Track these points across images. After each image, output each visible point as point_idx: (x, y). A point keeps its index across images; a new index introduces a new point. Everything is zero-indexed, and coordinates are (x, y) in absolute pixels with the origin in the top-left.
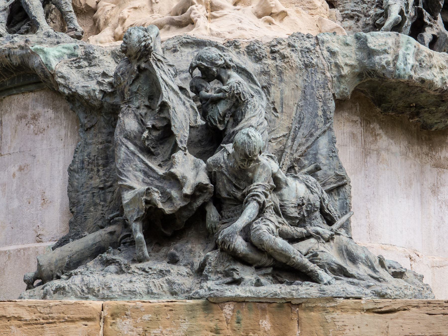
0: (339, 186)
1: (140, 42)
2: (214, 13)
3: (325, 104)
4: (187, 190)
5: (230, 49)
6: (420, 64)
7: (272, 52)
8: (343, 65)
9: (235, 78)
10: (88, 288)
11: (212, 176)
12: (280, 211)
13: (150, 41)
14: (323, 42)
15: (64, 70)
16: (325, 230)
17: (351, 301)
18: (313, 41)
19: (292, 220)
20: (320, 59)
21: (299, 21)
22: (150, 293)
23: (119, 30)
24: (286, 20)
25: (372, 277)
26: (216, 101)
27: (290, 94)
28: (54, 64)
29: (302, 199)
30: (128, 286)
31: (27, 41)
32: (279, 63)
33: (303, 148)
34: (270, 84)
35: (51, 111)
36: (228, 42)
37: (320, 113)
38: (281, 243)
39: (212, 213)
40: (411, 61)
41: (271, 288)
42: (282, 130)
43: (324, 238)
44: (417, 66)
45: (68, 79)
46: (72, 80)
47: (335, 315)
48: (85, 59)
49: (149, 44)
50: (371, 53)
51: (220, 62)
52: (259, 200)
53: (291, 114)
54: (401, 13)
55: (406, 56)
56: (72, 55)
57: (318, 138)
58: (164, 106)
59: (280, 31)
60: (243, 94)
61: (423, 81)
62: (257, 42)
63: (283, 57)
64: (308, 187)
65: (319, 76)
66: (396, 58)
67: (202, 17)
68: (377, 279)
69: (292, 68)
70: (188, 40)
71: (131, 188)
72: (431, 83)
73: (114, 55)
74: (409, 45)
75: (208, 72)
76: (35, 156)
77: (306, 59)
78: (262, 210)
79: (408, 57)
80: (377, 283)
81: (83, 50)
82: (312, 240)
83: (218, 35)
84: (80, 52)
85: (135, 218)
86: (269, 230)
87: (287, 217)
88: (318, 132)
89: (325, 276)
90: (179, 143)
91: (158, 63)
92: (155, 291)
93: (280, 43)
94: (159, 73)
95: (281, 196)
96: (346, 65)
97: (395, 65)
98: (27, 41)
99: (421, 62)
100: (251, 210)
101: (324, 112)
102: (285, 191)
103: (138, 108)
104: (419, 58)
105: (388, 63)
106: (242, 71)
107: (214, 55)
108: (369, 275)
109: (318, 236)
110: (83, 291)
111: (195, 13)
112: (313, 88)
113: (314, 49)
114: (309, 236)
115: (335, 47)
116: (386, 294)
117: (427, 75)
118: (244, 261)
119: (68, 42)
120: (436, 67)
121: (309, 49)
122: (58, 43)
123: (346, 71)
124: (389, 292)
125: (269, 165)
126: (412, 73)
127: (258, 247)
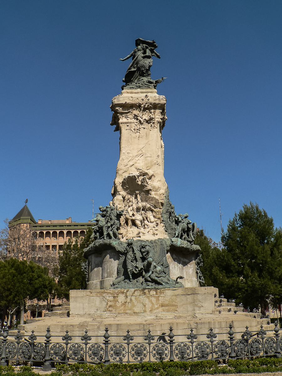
0: (168, 267)
4: (139, 269)
9: (147, 248)
11: (144, 266)
12: (156, 272)
15: (117, 246)
16: (164, 275)
23: (127, 238)
26: (144, 252)
33: (161, 260)
38: (156, 278)
39: (144, 273)
47: (166, 291)
50: (172, 242)
54: (178, 234)
55: (179, 242)
56: (118, 243)
58: (135, 254)
59: (156, 238)
66: (177, 243)
71: (129, 268)
73: (126, 243)
76: (112, 262)
78: (153, 272)
84: (120, 243)
86: (154, 276)
99: (182, 243)
100: (151, 272)
106: (148, 246)
118: (149, 281)
119: (117, 242)
125: (154, 264)
127: (152, 279)
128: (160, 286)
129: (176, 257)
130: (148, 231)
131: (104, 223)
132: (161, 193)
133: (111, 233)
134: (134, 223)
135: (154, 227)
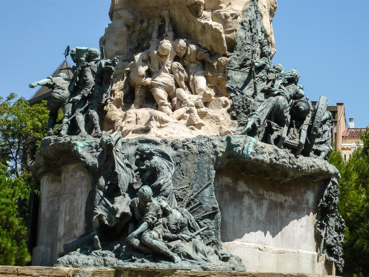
1: (107, 142)
2: (162, 125)
3: (209, 171)
5: (162, 144)
6: (256, 152)
7: (184, 145)
8: (219, 152)
9: (156, 159)
10: (69, 262)
13: (112, 142)
14: (211, 140)
17: (183, 271)
18: (206, 139)
19: (172, 231)
20: (208, 149)
21: (210, 128)
22: (95, 265)
24: (202, 128)
25: (204, 259)
27: (191, 166)
28: (80, 150)
29: (178, 220)
30: (86, 261)
31: (71, 139)
32: (186, 150)
34: (181, 161)
35: (83, 173)
36: (163, 140)
37: (206, 176)
40: (251, 150)
41: (148, 264)
42: (186, 184)
43: (185, 240)
44: (254, 153)
45: (86, 158)
46: (87, 158)
48: (95, 148)
49: (111, 143)
51: (148, 152)
52: (148, 221)
53: (191, 176)
57: (204, 189)
58: (116, 174)
60: (158, 168)
61: (257, 160)
62: (177, 140)
63: (188, 148)
64: (182, 215)
65: (206, 158)
66: (243, 149)
67: (154, 127)
68: (206, 261)
69: (192, 153)
70: (143, 139)
72: (262, 161)
74: (251, 142)
75: (143, 156)
76: (75, 195)
77: (200, 149)
79: (249, 148)
80: (206, 262)
81: (95, 144)
82: (179, 241)
83: (159, 136)
85: (96, 228)
87: (169, 228)
88: (204, 186)
89: (177, 258)
90: (121, 192)
91: (116, 153)
92: (97, 264)
93: (188, 141)
94: (116, 157)
95: (168, 218)
96: (221, 152)
97: (242, 152)
98: (71, 139)
100: (144, 226)
101: (208, 175)
102: (170, 216)
103: (107, 174)
104: (256, 148)
105: (239, 151)
107: (144, 148)
108: (202, 258)
109: (182, 239)
110: (67, 263)
111: (151, 125)
112: (203, 163)
113: (205, 144)
114: (178, 239)
115: (216, 143)
116: (207, 268)
117: (260, 157)
120: (266, 153)
121: (202, 144)
122: (84, 140)
123: (220, 155)
124: (209, 267)
126: (251, 156)
127: (143, 243)
128: (163, 265)
129: (247, 189)
130: (178, 116)
131: (66, 93)
132: (228, 14)
133: (81, 118)
134: (151, 92)
135: (197, 107)
